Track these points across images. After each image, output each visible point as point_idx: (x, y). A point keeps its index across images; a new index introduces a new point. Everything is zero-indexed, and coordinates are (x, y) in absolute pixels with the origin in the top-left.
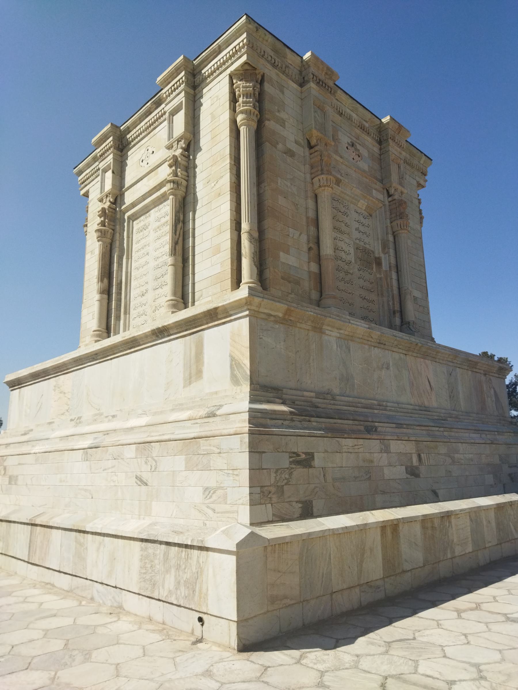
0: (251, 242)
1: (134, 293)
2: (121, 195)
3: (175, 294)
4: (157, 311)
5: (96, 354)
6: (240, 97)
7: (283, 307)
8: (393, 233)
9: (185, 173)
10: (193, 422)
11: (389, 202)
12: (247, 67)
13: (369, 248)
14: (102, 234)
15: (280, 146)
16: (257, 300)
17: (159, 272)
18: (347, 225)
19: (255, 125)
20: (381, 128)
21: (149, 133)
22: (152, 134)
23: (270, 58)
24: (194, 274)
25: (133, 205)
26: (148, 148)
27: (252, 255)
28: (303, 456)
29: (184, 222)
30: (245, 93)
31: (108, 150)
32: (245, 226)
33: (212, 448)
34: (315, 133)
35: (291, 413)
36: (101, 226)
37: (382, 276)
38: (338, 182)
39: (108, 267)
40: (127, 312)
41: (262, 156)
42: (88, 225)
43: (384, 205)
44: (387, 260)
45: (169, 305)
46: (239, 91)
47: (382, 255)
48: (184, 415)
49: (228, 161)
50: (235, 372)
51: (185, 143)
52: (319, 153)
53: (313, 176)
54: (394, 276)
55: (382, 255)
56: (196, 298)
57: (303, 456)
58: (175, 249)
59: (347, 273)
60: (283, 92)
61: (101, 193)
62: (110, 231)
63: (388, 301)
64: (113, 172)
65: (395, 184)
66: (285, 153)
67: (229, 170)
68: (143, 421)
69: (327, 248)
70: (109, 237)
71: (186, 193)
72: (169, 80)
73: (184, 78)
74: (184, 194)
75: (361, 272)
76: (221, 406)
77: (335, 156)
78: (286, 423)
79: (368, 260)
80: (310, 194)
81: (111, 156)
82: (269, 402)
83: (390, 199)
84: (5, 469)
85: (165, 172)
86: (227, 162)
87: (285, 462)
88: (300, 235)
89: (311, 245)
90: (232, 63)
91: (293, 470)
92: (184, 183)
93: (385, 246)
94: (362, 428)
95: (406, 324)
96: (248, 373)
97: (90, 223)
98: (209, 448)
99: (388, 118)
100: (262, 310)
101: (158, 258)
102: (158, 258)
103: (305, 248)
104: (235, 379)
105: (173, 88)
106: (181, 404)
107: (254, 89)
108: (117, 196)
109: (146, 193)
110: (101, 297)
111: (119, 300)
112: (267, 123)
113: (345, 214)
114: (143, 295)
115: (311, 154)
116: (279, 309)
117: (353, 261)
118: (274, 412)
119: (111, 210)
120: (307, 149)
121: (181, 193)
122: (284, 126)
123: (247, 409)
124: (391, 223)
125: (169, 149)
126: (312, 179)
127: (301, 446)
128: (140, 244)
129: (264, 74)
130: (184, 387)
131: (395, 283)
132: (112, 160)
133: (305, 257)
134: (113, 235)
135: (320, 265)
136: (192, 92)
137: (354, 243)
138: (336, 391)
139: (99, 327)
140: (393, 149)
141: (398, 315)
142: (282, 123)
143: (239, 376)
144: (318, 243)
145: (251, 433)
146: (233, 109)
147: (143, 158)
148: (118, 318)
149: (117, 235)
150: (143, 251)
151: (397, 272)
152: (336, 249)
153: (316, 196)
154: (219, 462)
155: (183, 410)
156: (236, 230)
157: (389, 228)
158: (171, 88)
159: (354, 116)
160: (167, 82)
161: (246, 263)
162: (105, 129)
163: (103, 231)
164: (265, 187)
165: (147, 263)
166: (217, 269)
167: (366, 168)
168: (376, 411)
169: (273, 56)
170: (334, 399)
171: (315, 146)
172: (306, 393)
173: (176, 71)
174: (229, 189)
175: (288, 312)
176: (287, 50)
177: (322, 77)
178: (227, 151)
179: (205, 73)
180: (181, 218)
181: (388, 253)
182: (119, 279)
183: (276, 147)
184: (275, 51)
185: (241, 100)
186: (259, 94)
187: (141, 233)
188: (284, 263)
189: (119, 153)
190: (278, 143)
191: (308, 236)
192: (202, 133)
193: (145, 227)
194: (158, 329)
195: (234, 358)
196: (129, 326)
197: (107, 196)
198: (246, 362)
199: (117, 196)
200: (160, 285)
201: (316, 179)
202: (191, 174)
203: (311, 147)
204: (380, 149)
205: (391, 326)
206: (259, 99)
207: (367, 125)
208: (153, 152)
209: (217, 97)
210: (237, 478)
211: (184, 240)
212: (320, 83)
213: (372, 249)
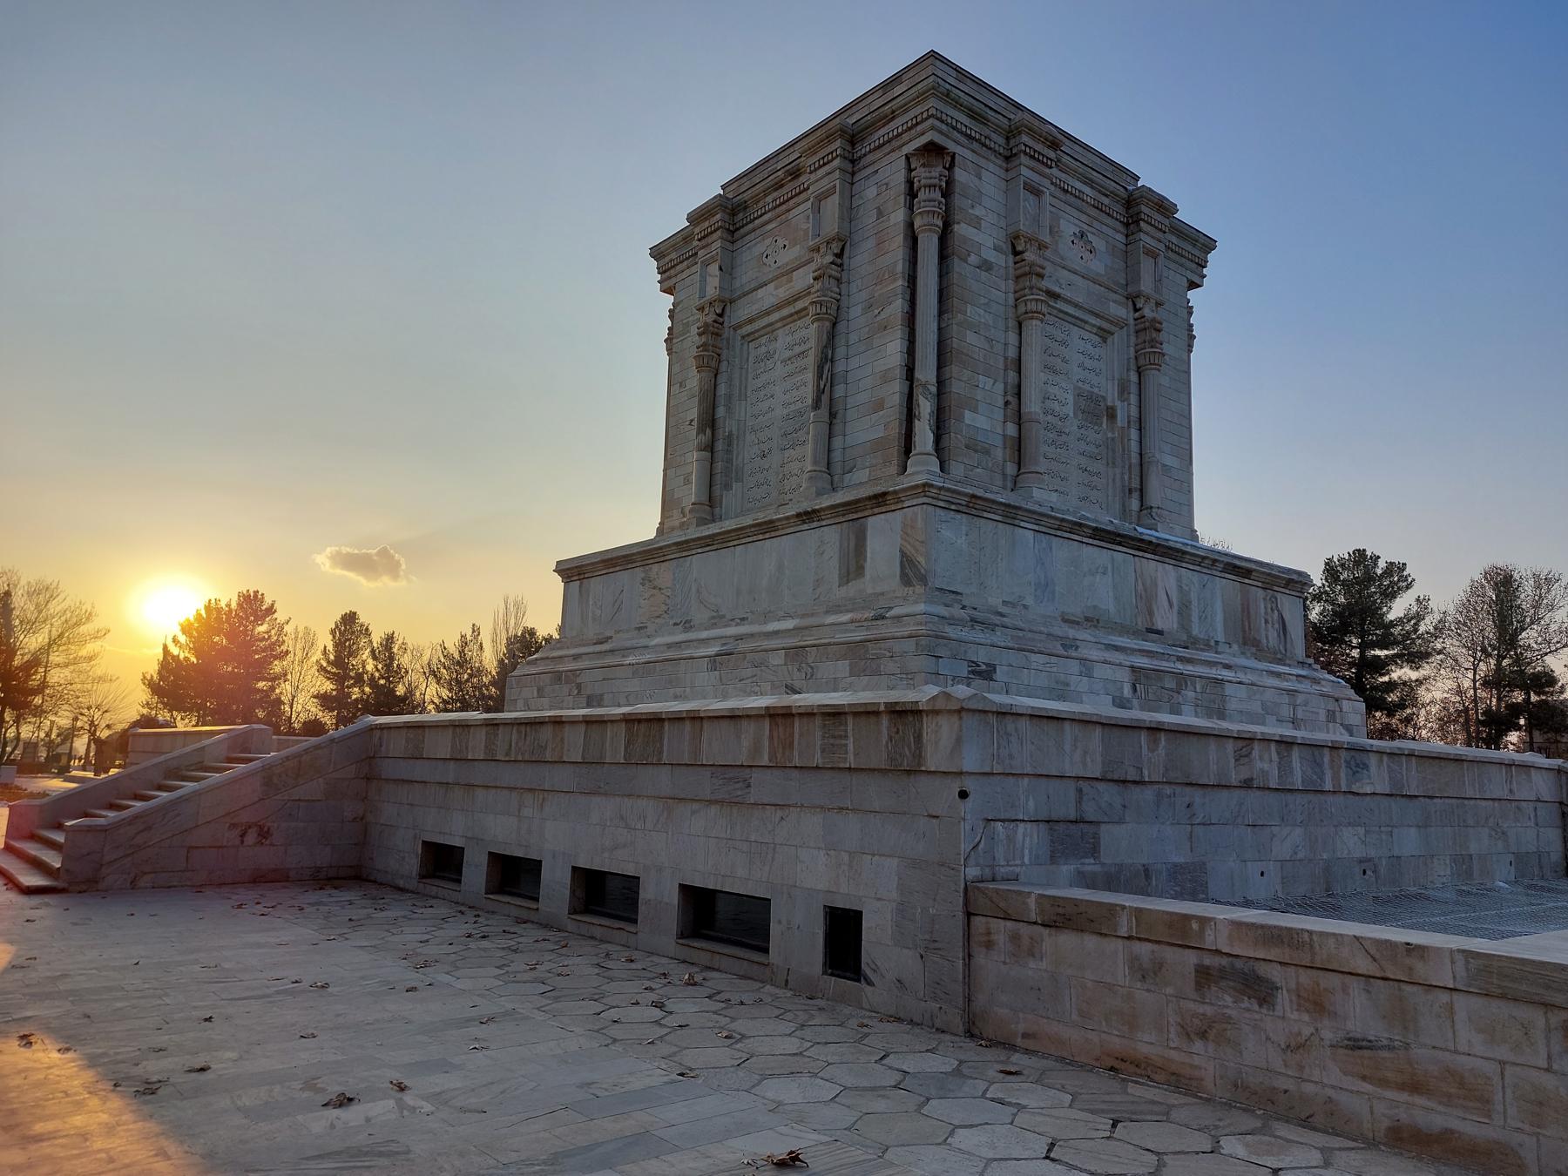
44: (1126, 411)
47: (1118, 404)
54: (1134, 434)
55: (1118, 404)
59: (1060, 433)
61: (701, 298)
69: (1032, 405)
84: (579, 686)
85: (803, 279)
89: (1010, 398)
93: (1123, 390)
103: (1001, 403)
113: (1063, 343)
131: (1134, 446)
133: (999, 415)
137: (1076, 388)
141: (1136, 495)
144: (1019, 394)
157: (1133, 361)
181: (1128, 399)
191: (1006, 384)
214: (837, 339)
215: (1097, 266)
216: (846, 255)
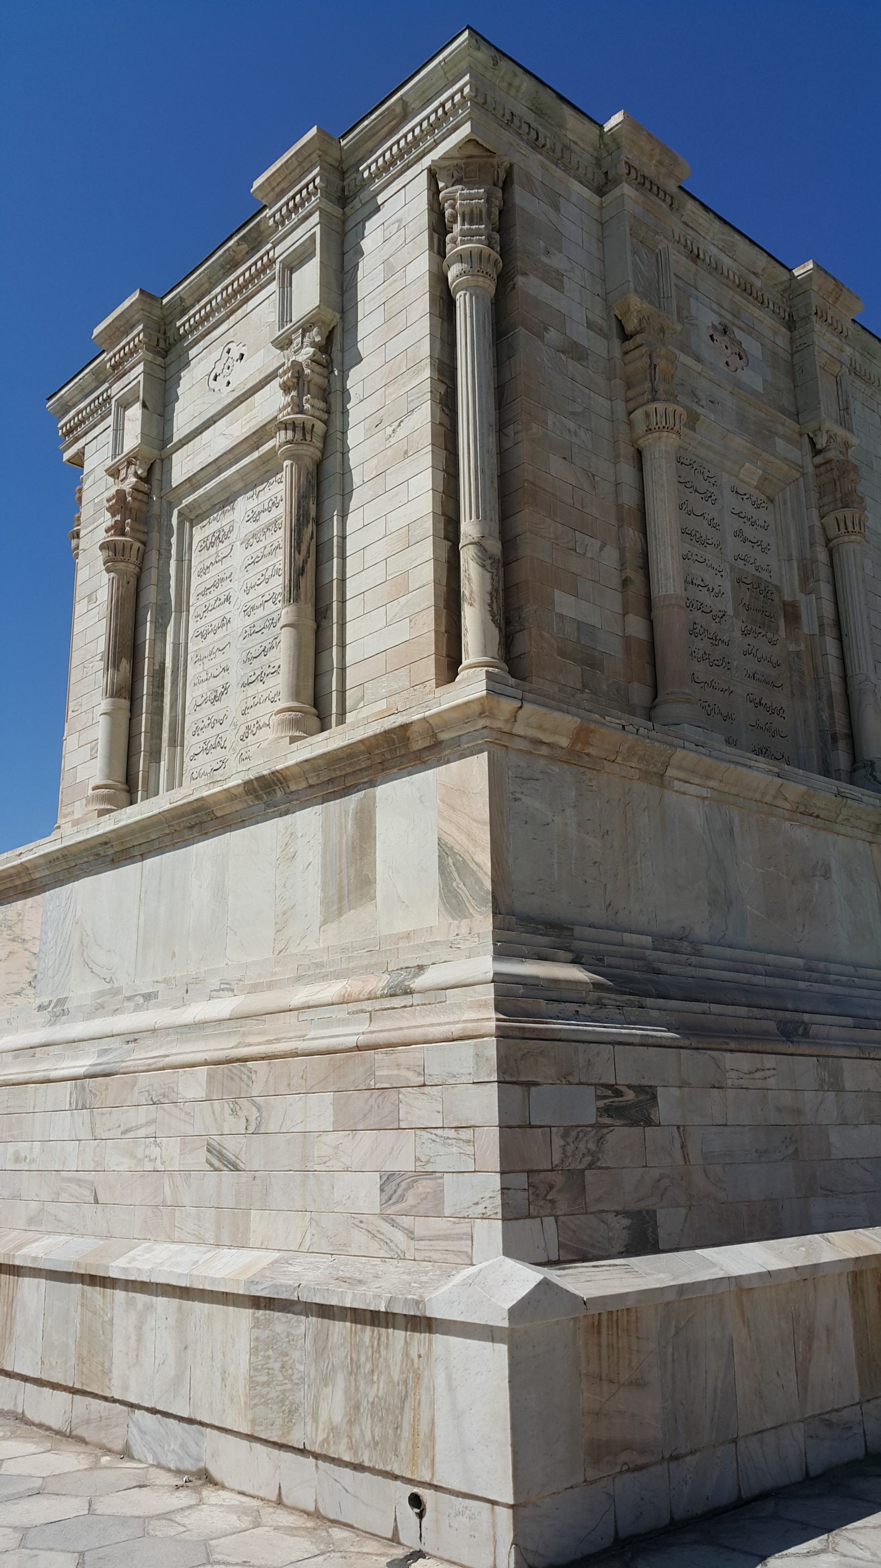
0: (483, 566)
1: (193, 694)
2: (162, 460)
3: (296, 694)
4: (251, 736)
5: (106, 843)
6: (455, 222)
7: (569, 722)
8: (828, 541)
9: (322, 405)
10: (352, 1007)
11: (817, 467)
12: (471, 150)
13: (768, 579)
14: (114, 552)
15: (552, 335)
16: (508, 706)
17: (256, 642)
18: (713, 524)
19: (490, 286)
20: (794, 290)
21: (233, 312)
22: (239, 313)
23: (525, 128)
24: (343, 646)
25: (193, 483)
26: (229, 346)
27: (488, 599)
28: (630, 1095)
29: (319, 522)
30: (467, 210)
31: (132, 353)
32: (469, 528)
33: (404, 1072)
34: (636, 302)
35: (596, 985)
36: (115, 534)
37: (803, 647)
38: (693, 420)
39: (130, 633)
40: (176, 741)
41: (509, 358)
42: (82, 534)
43: (803, 475)
44: (815, 608)
45: (282, 722)
46: (453, 206)
47: (801, 598)
48: (331, 990)
49: (427, 373)
50: (455, 884)
51: (319, 333)
52: (644, 349)
53: (631, 405)
54: (831, 645)
55: (801, 598)
56: (349, 703)
57: (630, 1095)
58: (298, 586)
59: (715, 640)
60: (557, 209)
61: (114, 455)
62: (137, 545)
63: (818, 711)
64: (144, 406)
65: (829, 425)
66: (563, 352)
67: (429, 396)
68: (223, 1007)
70: (133, 559)
71: (323, 451)
72: (283, 185)
73: (318, 180)
74: (319, 454)
75: (749, 639)
76: (421, 968)
77: (682, 357)
78: (586, 1010)
79: (766, 608)
80: (626, 450)
81: (140, 368)
82: (541, 958)
83: (819, 459)
85: (273, 402)
86: (424, 375)
87: (587, 1110)
88: (601, 549)
89: (630, 572)
90: (436, 144)
91: (605, 1131)
92: (320, 427)
93: (807, 577)
94: (772, 1026)
95: (865, 767)
96: (488, 885)
97: (86, 528)
98: (395, 1072)
99: (810, 265)
100: (519, 729)
101: (253, 608)
102: (253, 608)
103: (615, 581)
104: (454, 901)
105: (291, 204)
106: (322, 965)
107: (488, 201)
108: (153, 462)
109: (225, 453)
110: (113, 704)
111: (157, 712)
112: (520, 280)
113: (708, 497)
114: (216, 699)
115: (626, 353)
116: (560, 727)
117: (730, 612)
118: (556, 982)
119: (140, 496)
120: (616, 342)
121: (311, 451)
122: (560, 288)
123: (490, 976)
124: (822, 517)
125: (282, 348)
126: (630, 413)
127: (625, 1071)
128: (208, 576)
129: (511, 165)
130: (324, 922)
132: (141, 378)
133: (613, 602)
134: (143, 556)
135: (652, 622)
136: (336, 211)
137: (733, 568)
138: (701, 931)
139: (109, 777)
140: (823, 339)
141: (842, 744)
142: (555, 279)
143: (464, 892)
144: (645, 568)
145: (502, 1035)
146: (439, 249)
147: (217, 371)
148: (155, 755)
149: (154, 555)
150: (215, 593)
151: (840, 639)
152: (689, 582)
153: (639, 453)
154: (419, 1108)
155: (325, 978)
156: (446, 538)
157: (818, 530)
158: (287, 204)
159: (727, 261)
160: (277, 190)
161: (472, 617)
162: (127, 303)
163: (119, 547)
164: (515, 434)
165: (225, 622)
166: (402, 633)
167: (758, 384)
168: (802, 985)
169: (533, 125)
170: (697, 953)
171: (637, 333)
172: (628, 937)
173: (300, 163)
174: (429, 440)
175: (582, 735)
176: (567, 110)
177: (650, 170)
178: (425, 349)
179: (369, 167)
180: (313, 513)
182: (158, 660)
183: (542, 339)
184: (538, 111)
185: (457, 228)
186: (501, 212)
187: (213, 550)
188: (562, 617)
189: (159, 360)
190: (546, 329)
191: (622, 550)
192: (363, 309)
193: (219, 538)
194: (261, 779)
195: (451, 848)
196: (182, 775)
197: (129, 463)
198: (482, 859)
199: (153, 462)
200: (258, 673)
201: (638, 414)
202: (337, 408)
203: (625, 337)
204: (792, 340)
205: (826, 772)
206: (501, 224)
207: (758, 283)
208: (242, 355)
209: (399, 221)
210: (469, 1150)
211: (318, 564)
212: (644, 183)
213: (776, 582)
214: (325, 485)
215: (753, 379)
216: (337, 346)
